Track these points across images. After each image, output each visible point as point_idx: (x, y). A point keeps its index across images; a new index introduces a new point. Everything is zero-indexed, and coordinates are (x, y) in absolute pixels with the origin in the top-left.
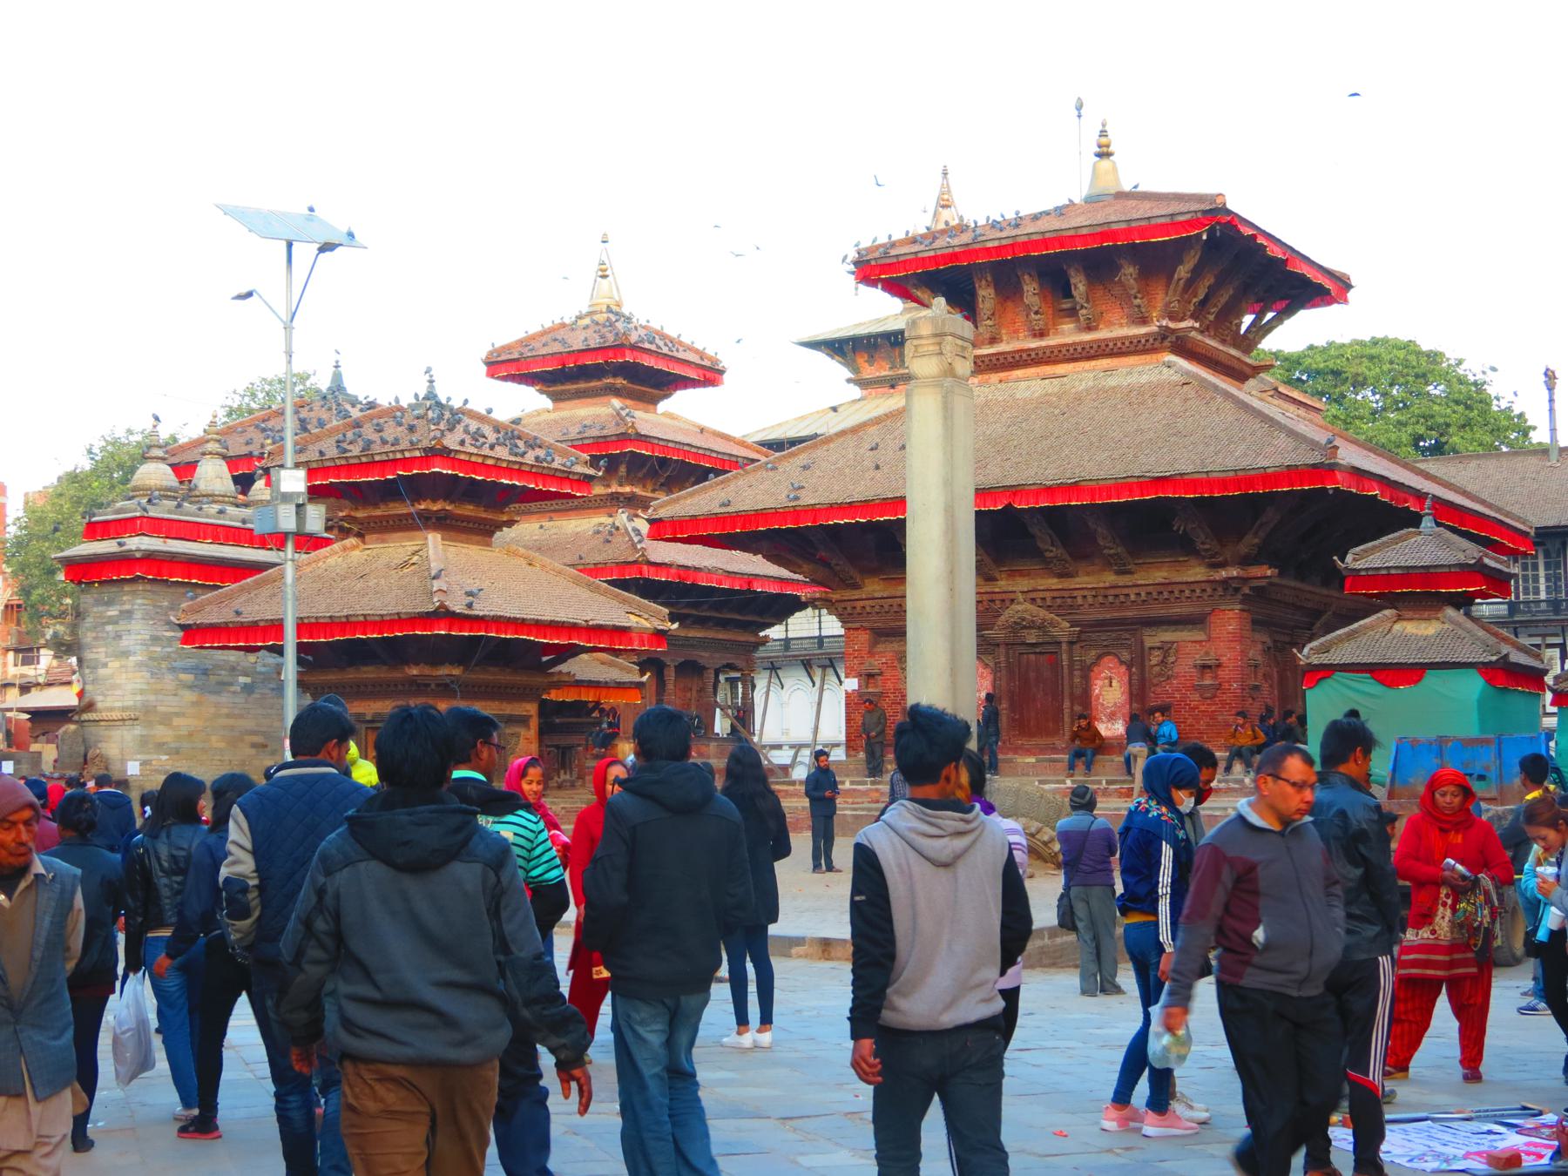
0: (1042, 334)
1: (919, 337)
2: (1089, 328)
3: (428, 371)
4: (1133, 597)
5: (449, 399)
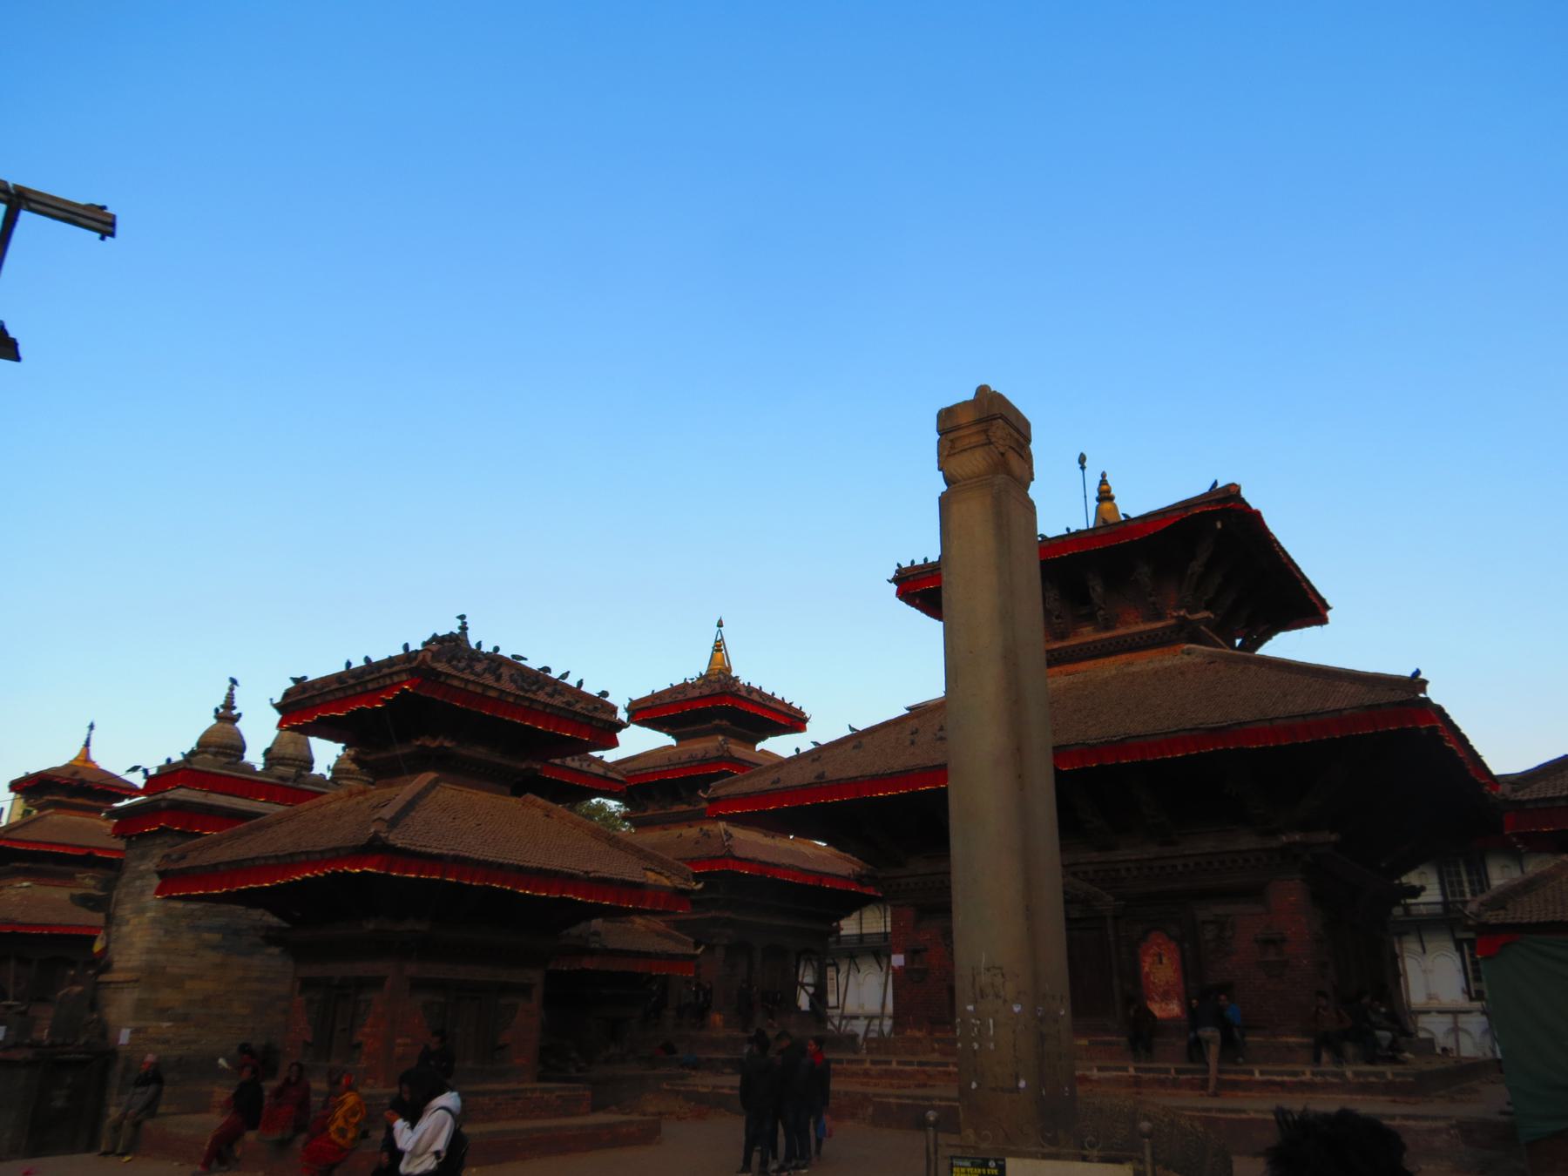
0: (1063, 637)
1: (958, 428)
2: (1107, 628)
3: (462, 617)
4: (1180, 868)
5: (479, 645)
